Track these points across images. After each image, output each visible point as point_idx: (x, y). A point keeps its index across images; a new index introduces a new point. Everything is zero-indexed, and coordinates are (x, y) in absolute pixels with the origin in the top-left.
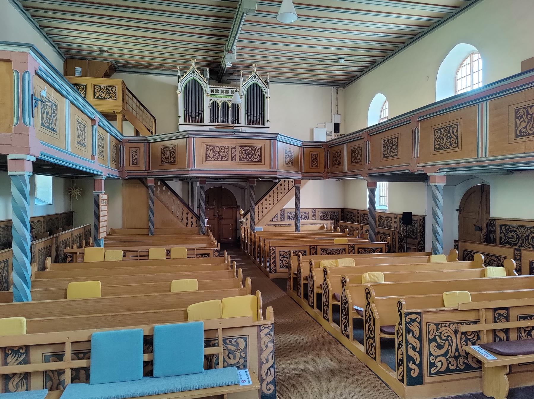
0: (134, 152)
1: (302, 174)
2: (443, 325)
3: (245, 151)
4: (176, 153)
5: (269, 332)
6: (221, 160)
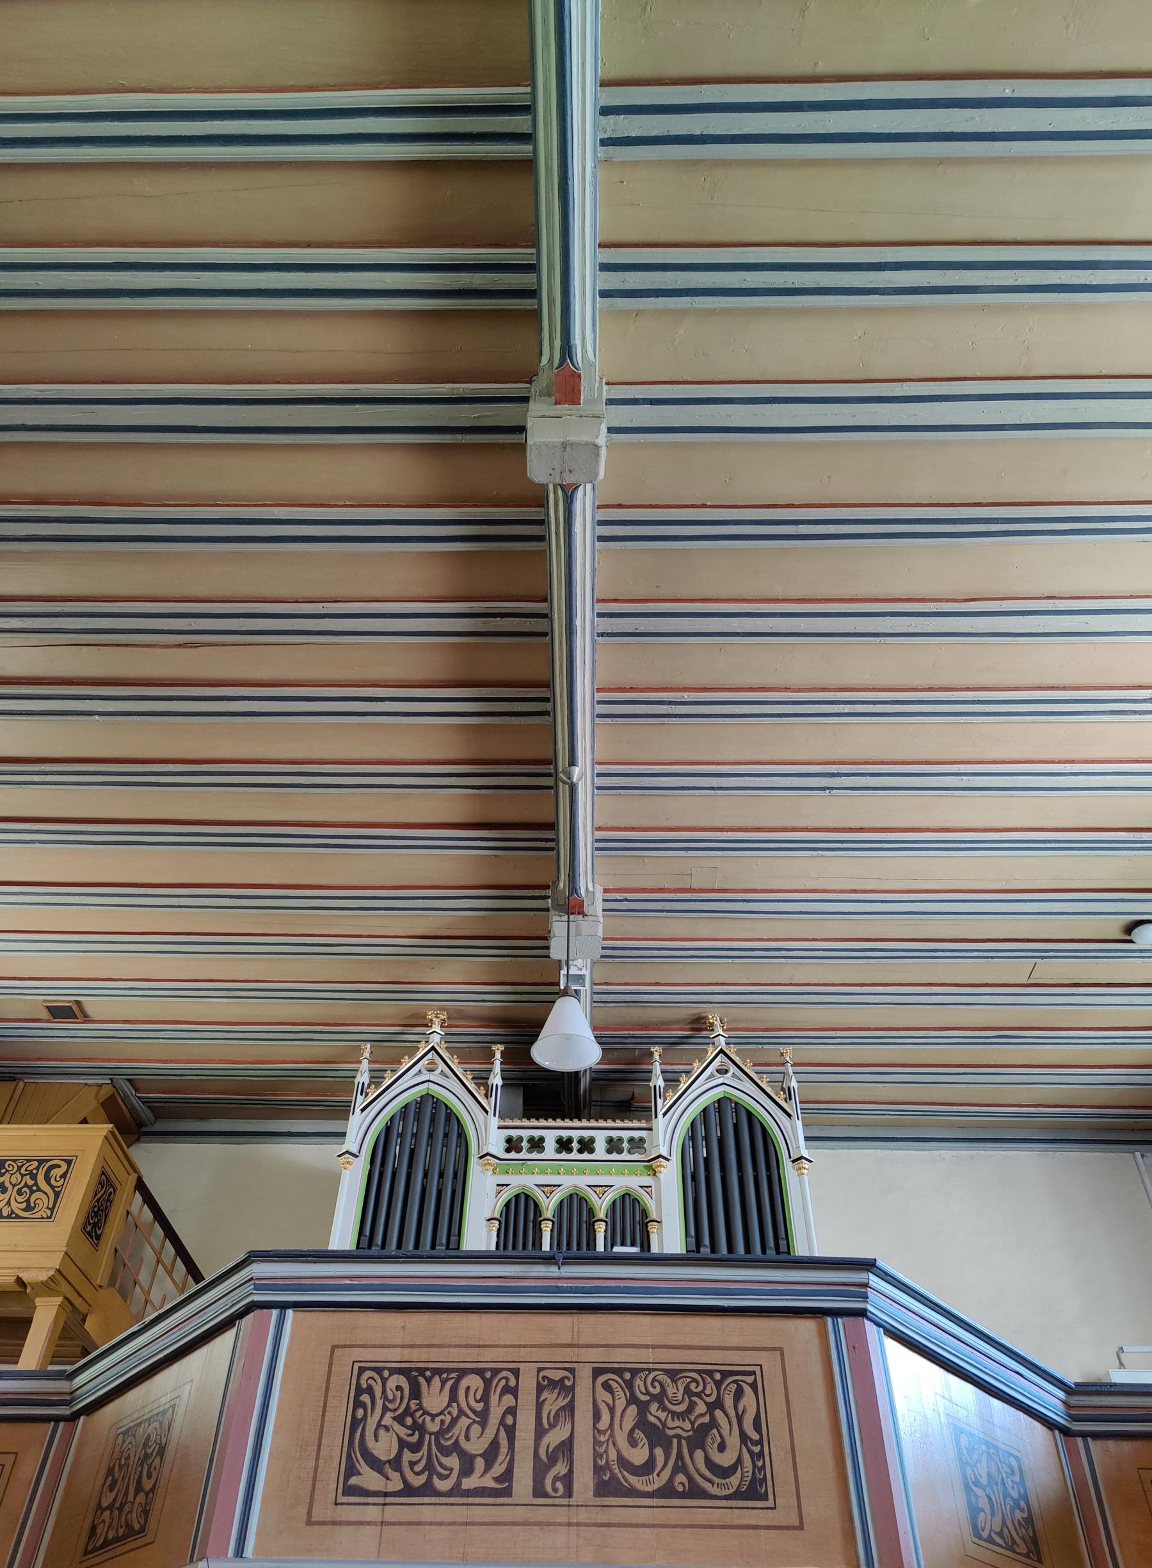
3: (643, 1408)
6: (456, 1491)
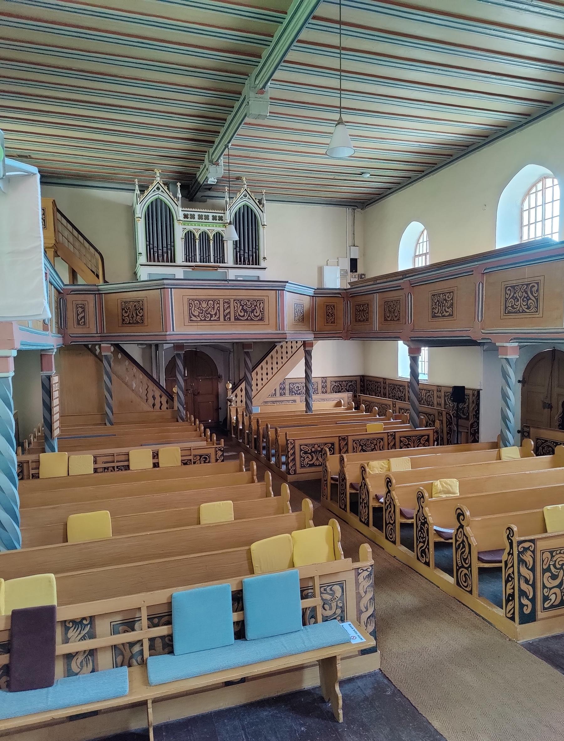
0: (80, 307)
1: (314, 334)
2: (558, 552)
3: (243, 306)
4: (145, 309)
5: (369, 575)
6: (210, 320)
